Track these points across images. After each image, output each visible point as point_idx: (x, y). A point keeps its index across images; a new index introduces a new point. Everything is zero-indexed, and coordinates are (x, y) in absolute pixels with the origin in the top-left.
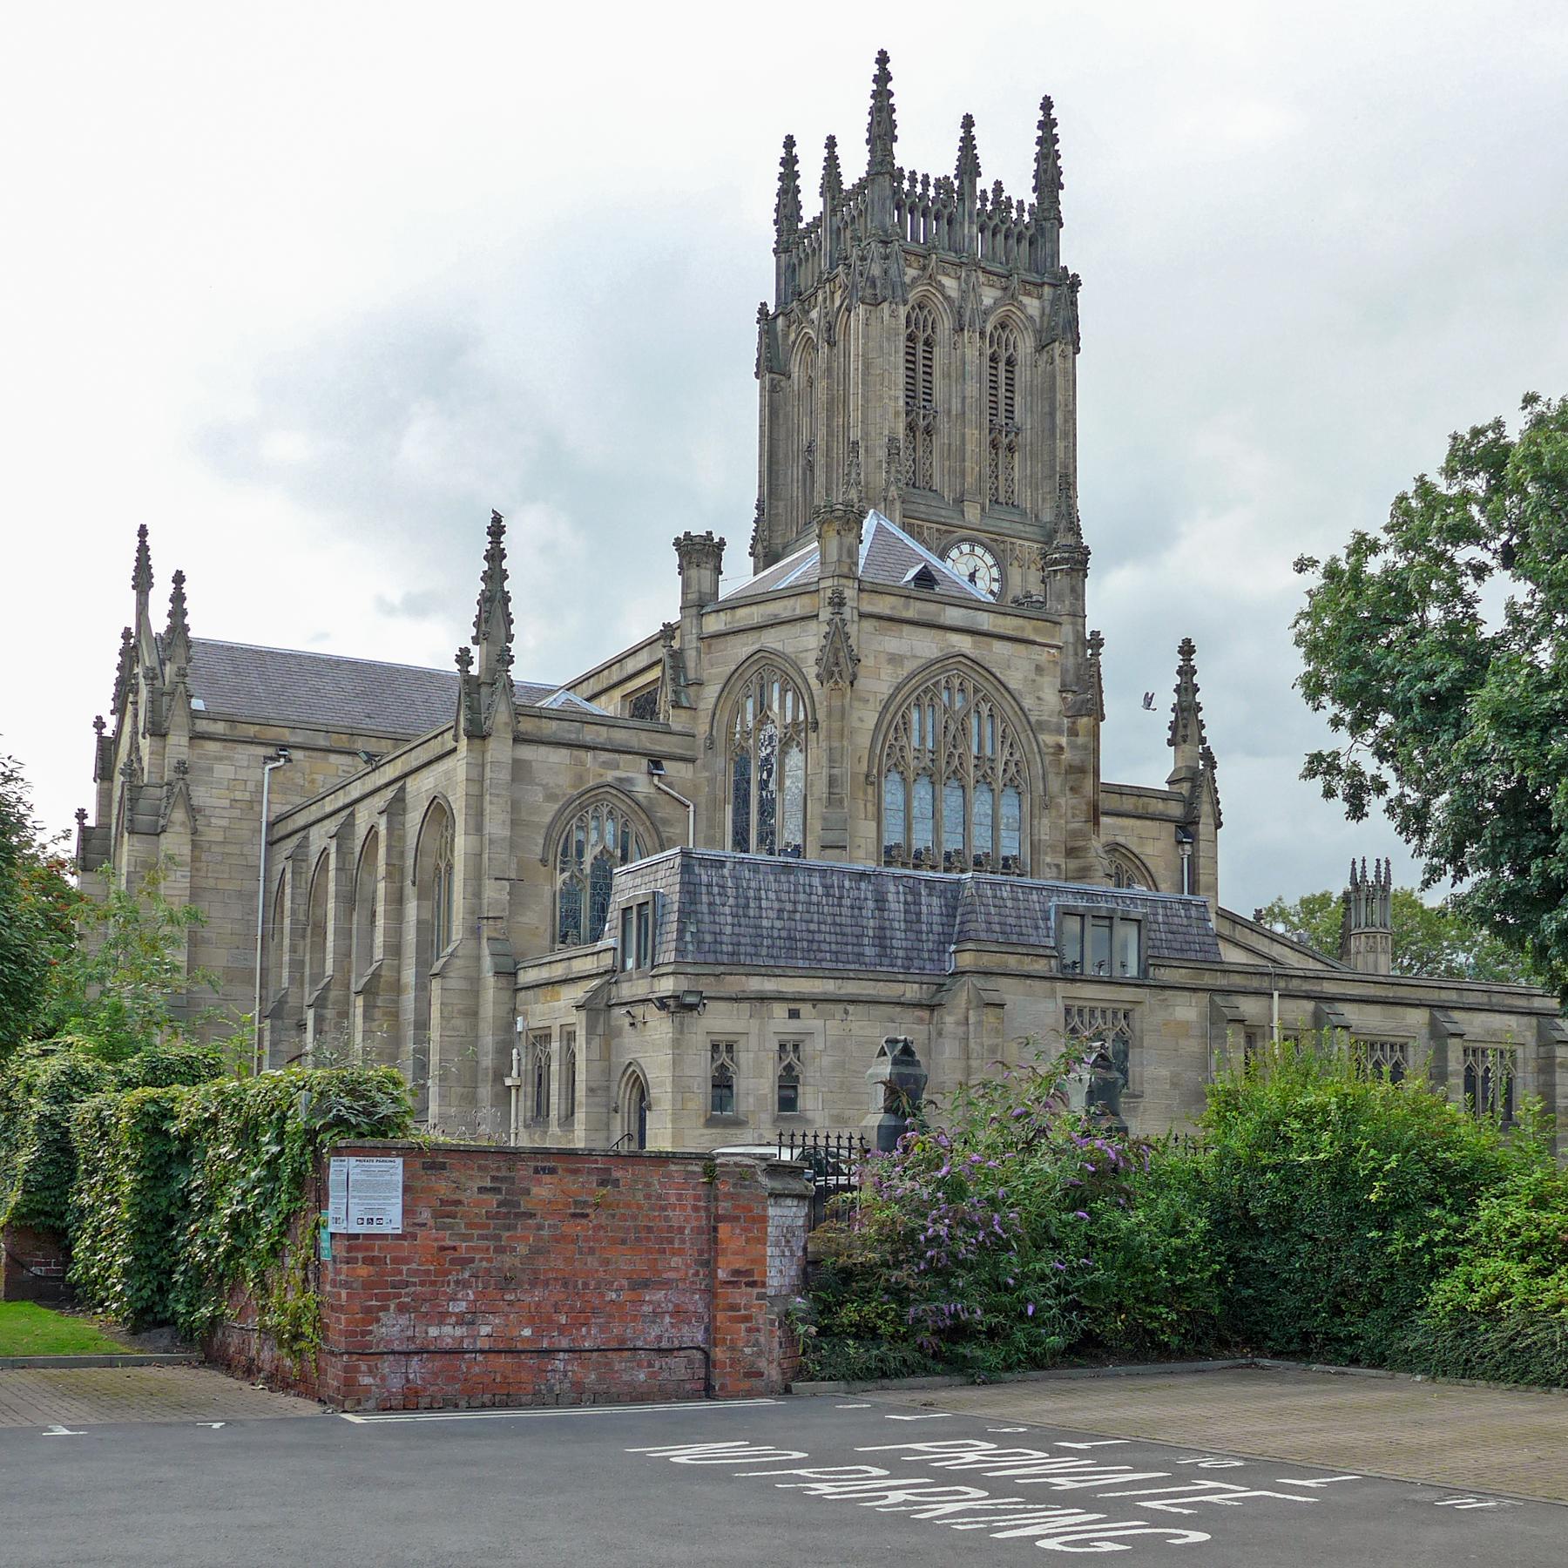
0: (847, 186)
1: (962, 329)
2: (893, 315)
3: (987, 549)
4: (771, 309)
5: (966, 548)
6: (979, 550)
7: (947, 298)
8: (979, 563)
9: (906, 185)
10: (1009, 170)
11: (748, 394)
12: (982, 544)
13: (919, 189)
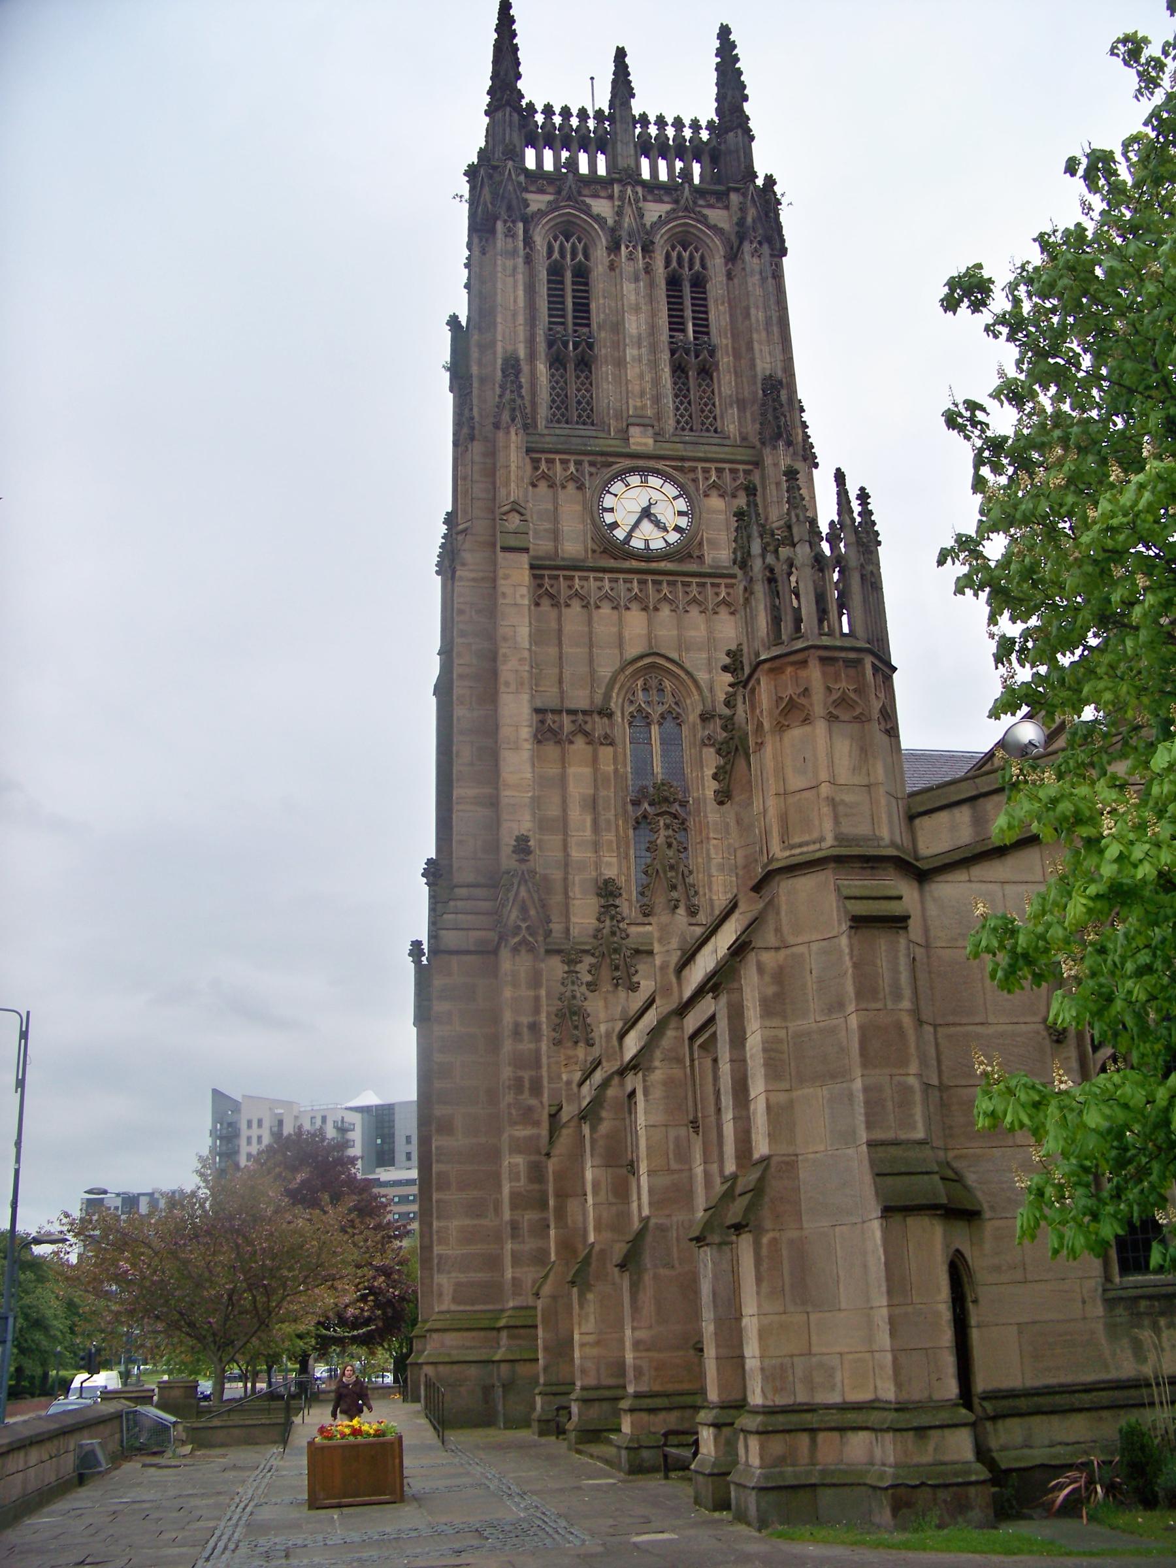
1: (618, 248)
2: (510, 234)
3: (667, 477)
5: (634, 480)
6: (654, 481)
7: (599, 219)
8: (656, 496)
9: (540, 118)
10: (677, 94)
12: (657, 472)
13: (557, 120)
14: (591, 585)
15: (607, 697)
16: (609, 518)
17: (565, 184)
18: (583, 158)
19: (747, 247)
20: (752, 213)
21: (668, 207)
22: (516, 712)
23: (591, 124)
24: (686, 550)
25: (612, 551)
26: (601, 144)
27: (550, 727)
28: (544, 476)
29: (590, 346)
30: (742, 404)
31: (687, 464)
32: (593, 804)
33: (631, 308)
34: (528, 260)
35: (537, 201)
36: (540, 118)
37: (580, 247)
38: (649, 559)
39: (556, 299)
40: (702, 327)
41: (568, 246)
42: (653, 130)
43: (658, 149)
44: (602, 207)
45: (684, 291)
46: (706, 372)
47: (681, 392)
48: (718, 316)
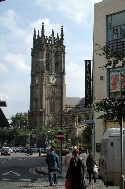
0: (40, 36)
4: (33, 48)
5: (52, 77)
11: (31, 57)
15: (49, 96)
22: (44, 98)
24: (56, 83)
36: (46, 37)
45: (57, 55)
48: (59, 60)
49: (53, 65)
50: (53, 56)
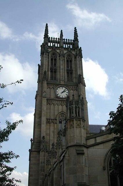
2: (46, 55)
5: (61, 88)
7: (58, 52)
9: (51, 39)
14: (55, 102)
15: (56, 117)
16: (57, 93)
17: (53, 48)
18: (56, 44)
19: (77, 57)
20: (78, 52)
21: (67, 51)
22: (44, 119)
23: (57, 40)
25: (57, 98)
26: (58, 43)
27: (48, 121)
28: (49, 87)
29: (56, 70)
30: (76, 78)
31: (68, 86)
32: (54, 132)
33: (62, 65)
34: (48, 58)
35: (50, 50)
36: (51, 39)
37: (55, 56)
38: (63, 99)
39: (52, 63)
40: (71, 67)
41: (54, 56)
42: (65, 41)
43: (66, 43)
44: (58, 51)
45: (69, 61)
46: (71, 73)
47: (68, 76)
48: (73, 66)
49: (62, 73)
50: (62, 61)
